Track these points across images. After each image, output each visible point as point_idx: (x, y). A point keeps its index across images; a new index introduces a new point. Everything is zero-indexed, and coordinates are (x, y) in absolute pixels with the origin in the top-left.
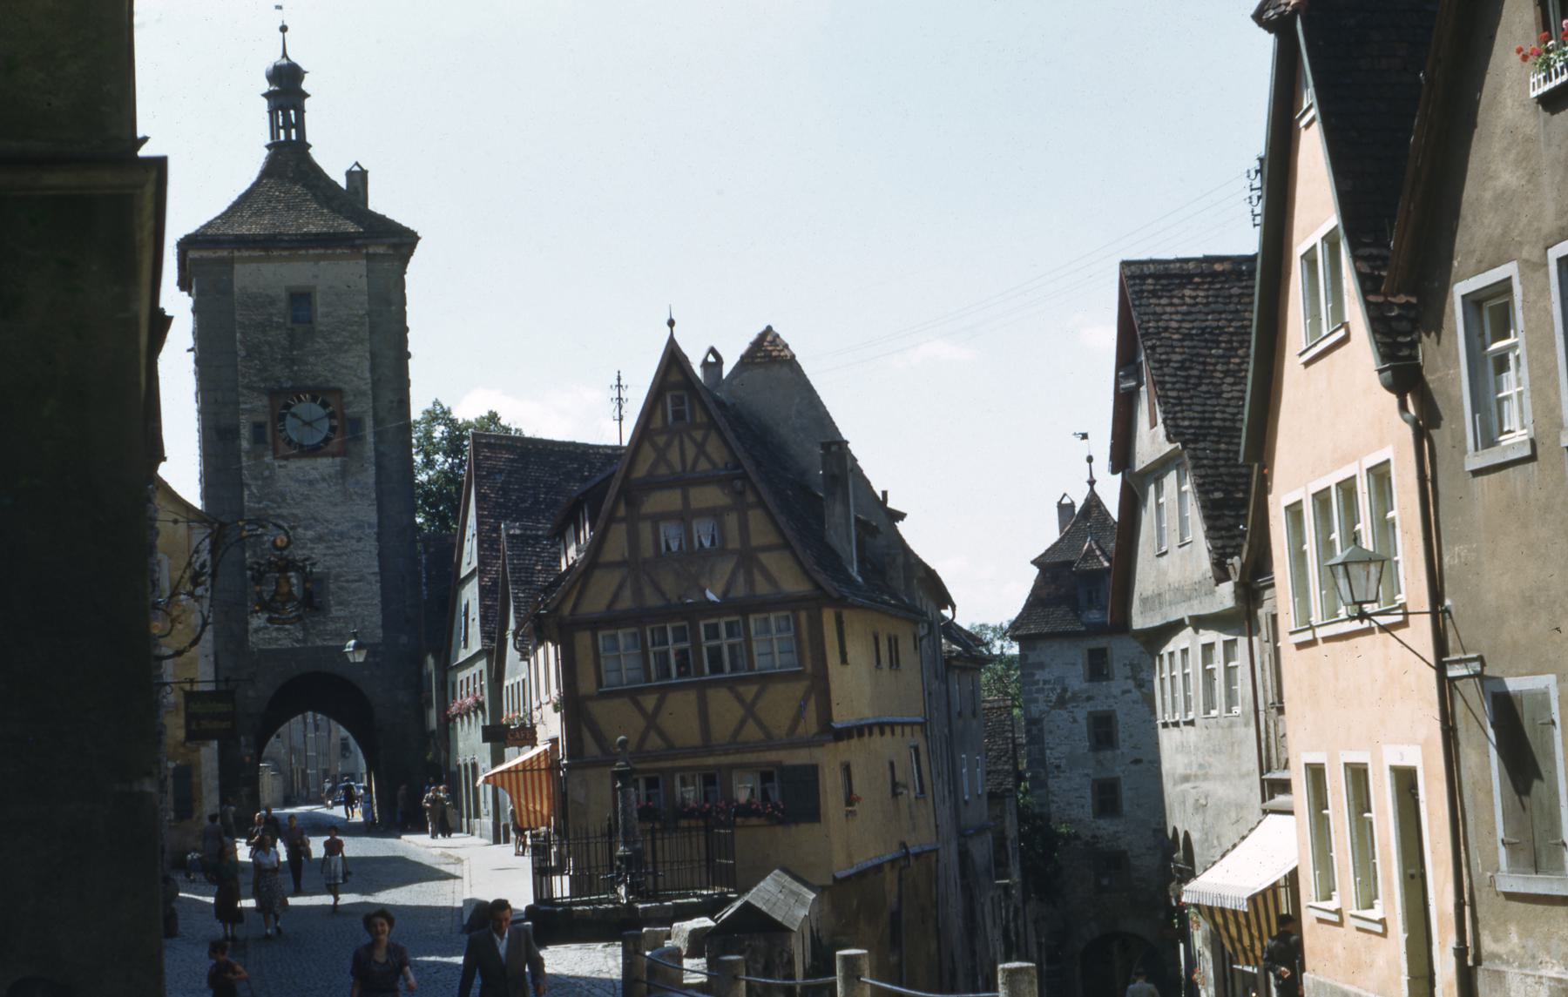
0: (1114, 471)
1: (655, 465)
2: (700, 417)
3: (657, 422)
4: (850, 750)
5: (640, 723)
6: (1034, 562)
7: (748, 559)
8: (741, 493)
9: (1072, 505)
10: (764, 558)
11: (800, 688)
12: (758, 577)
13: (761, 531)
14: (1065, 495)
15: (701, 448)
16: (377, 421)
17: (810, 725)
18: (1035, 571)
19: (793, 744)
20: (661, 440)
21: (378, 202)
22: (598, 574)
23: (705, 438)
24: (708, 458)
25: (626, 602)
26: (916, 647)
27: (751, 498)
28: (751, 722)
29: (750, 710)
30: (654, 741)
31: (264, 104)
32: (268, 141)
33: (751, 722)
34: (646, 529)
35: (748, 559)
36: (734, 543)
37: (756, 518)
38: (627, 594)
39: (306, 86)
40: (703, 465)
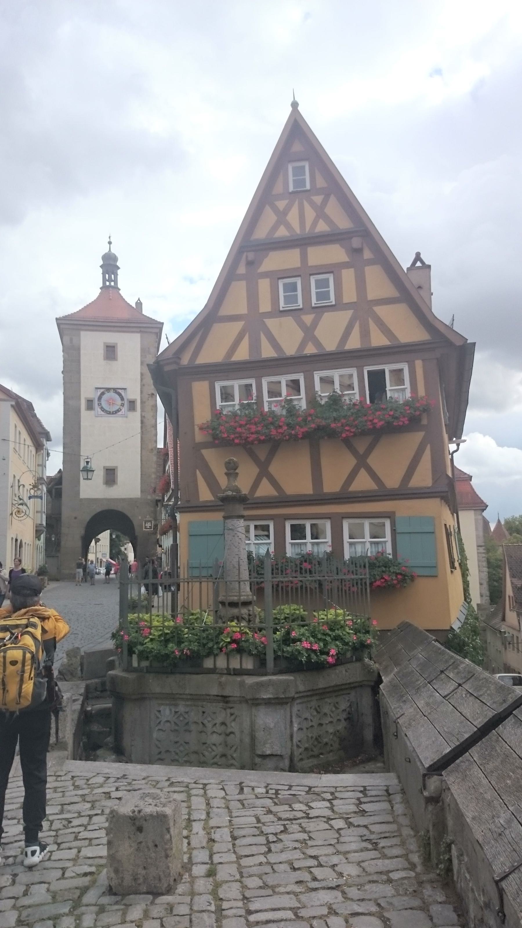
1: (275, 228)
2: (321, 183)
10: (381, 311)
12: (373, 326)
15: (321, 214)
16: (142, 402)
20: (281, 205)
21: (147, 311)
23: (325, 202)
27: (367, 254)
31: (101, 271)
32: (101, 285)
33: (363, 473)
34: (264, 285)
38: (245, 344)
39: (118, 264)
40: (322, 227)
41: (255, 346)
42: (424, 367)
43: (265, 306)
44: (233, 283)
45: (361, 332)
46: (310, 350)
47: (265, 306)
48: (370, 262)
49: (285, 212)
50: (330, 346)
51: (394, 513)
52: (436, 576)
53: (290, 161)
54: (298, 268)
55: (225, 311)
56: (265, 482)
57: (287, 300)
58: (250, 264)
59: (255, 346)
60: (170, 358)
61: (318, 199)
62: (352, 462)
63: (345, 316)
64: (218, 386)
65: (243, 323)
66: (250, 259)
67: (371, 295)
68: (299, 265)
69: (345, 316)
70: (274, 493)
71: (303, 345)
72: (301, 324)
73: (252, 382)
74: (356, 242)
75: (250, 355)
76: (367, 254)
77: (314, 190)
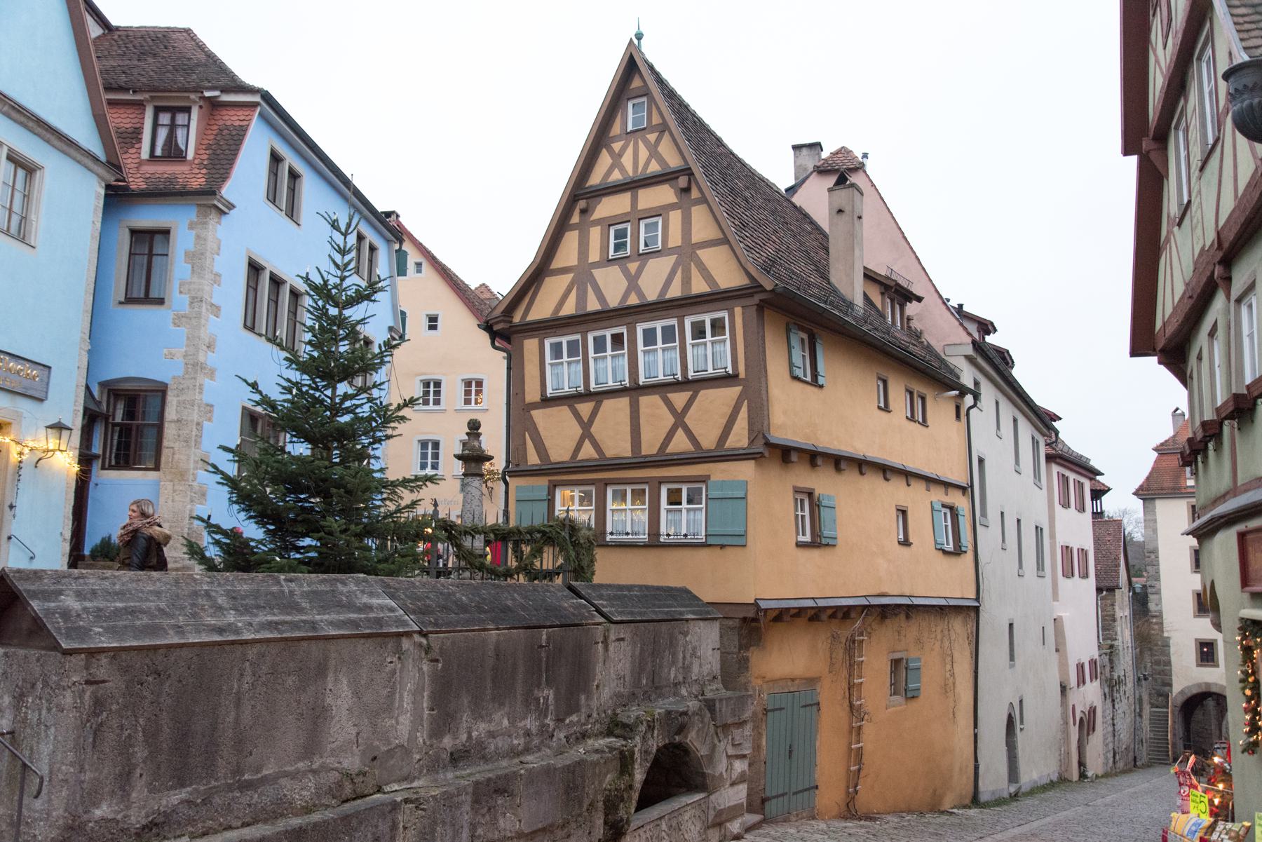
0: (1127, 152)
3: (616, 129)
4: (823, 483)
5: (578, 431)
6: (1155, 450)
7: (687, 253)
8: (687, 190)
9: (1183, 414)
10: (703, 254)
11: (734, 392)
12: (695, 272)
13: (703, 227)
14: (1177, 409)
15: (654, 153)
17: (739, 438)
18: (1156, 454)
19: (722, 456)
20: (617, 146)
22: (548, 280)
23: (658, 140)
24: (661, 160)
25: (569, 309)
26: (958, 416)
28: (680, 433)
29: (680, 419)
30: (588, 452)
33: (680, 433)
34: (595, 233)
35: (687, 253)
36: (675, 240)
37: (699, 214)
40: (654, 168)
41: (582, 299)
42: (743, 313)
43: (594, 256)
44: (567, 234)
45: (683, 278)
46: (633, 300)
47: (594, 256)
48: (698, 202)
49: (620, 155)
50: (652, 295)
51: (709, 477)
52: (745, 546)
53: (629, 99)
54: (628, 213)
55: (557, 264)
56: (587, 442)
57: (618, 247)
58: (584, 212)
59: (582, 299)
60: (499, 317)
61: (652, 137)
62: (670, 420)
63: (667, 262)
64: (547, 343)
65: (572, 275)
66: (581, 207)
67: (695, 239)
68: (629, 210)
69: (670, 260)
70: (596, 456)
71: (626, 296)
72: (626, 272)
73: (578, 337)
74: (682, 182)
75: (576, 311)
76: (695, 194)
77: (650, 128)
